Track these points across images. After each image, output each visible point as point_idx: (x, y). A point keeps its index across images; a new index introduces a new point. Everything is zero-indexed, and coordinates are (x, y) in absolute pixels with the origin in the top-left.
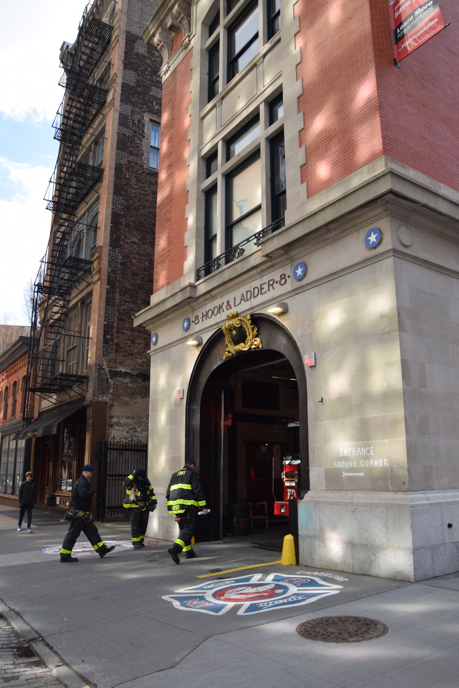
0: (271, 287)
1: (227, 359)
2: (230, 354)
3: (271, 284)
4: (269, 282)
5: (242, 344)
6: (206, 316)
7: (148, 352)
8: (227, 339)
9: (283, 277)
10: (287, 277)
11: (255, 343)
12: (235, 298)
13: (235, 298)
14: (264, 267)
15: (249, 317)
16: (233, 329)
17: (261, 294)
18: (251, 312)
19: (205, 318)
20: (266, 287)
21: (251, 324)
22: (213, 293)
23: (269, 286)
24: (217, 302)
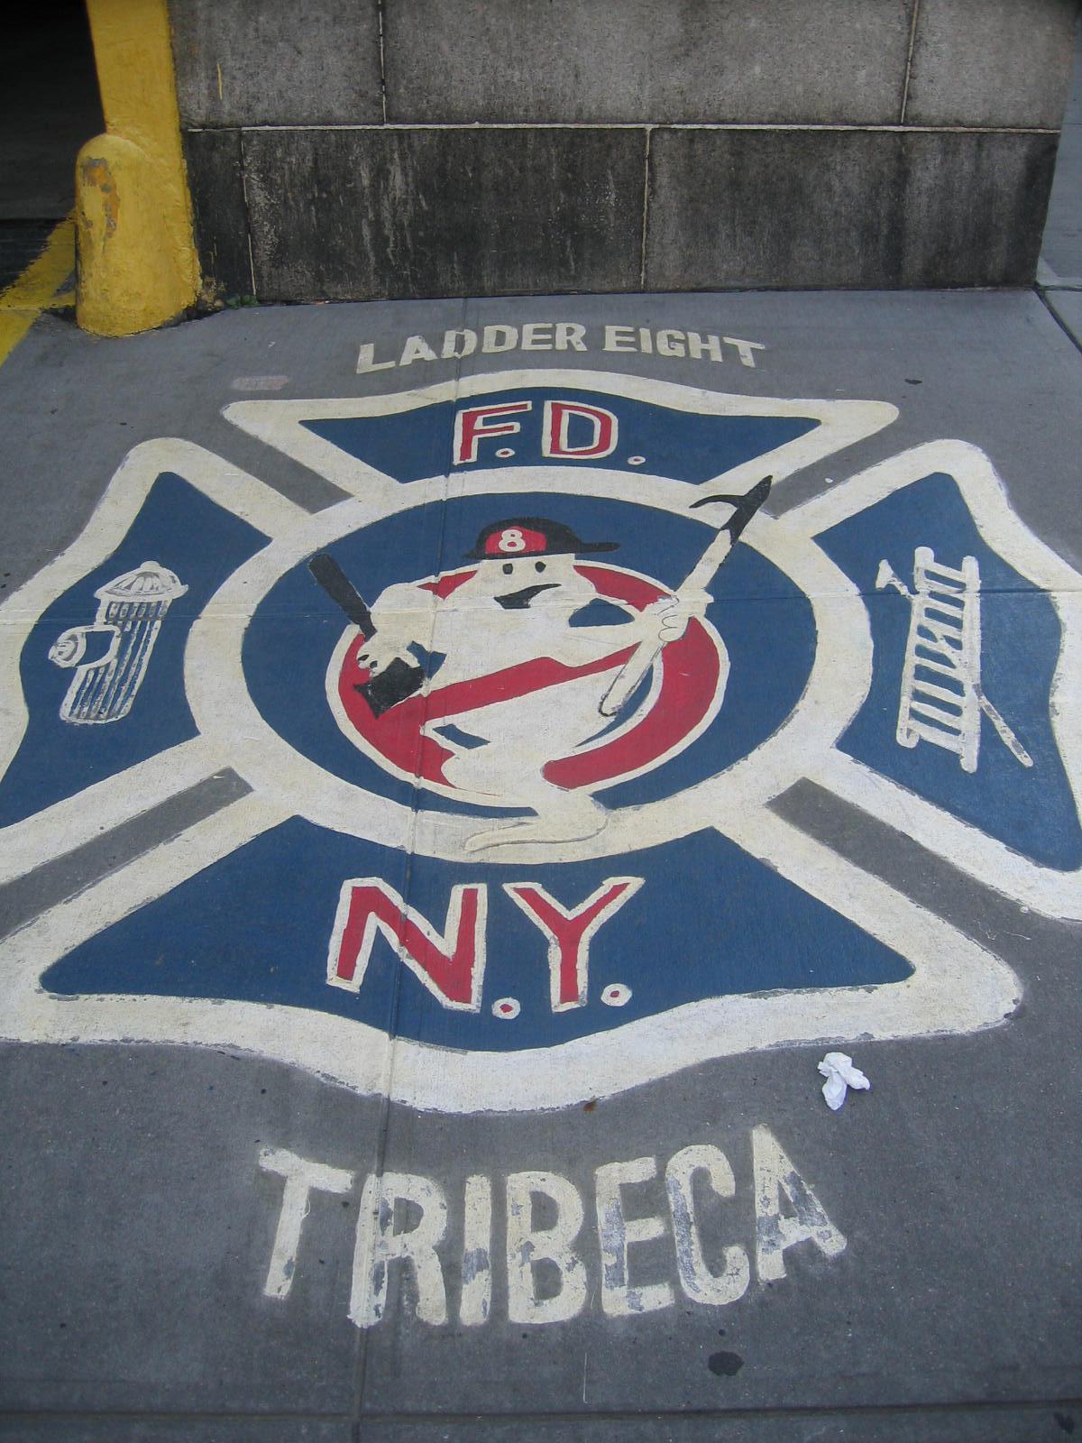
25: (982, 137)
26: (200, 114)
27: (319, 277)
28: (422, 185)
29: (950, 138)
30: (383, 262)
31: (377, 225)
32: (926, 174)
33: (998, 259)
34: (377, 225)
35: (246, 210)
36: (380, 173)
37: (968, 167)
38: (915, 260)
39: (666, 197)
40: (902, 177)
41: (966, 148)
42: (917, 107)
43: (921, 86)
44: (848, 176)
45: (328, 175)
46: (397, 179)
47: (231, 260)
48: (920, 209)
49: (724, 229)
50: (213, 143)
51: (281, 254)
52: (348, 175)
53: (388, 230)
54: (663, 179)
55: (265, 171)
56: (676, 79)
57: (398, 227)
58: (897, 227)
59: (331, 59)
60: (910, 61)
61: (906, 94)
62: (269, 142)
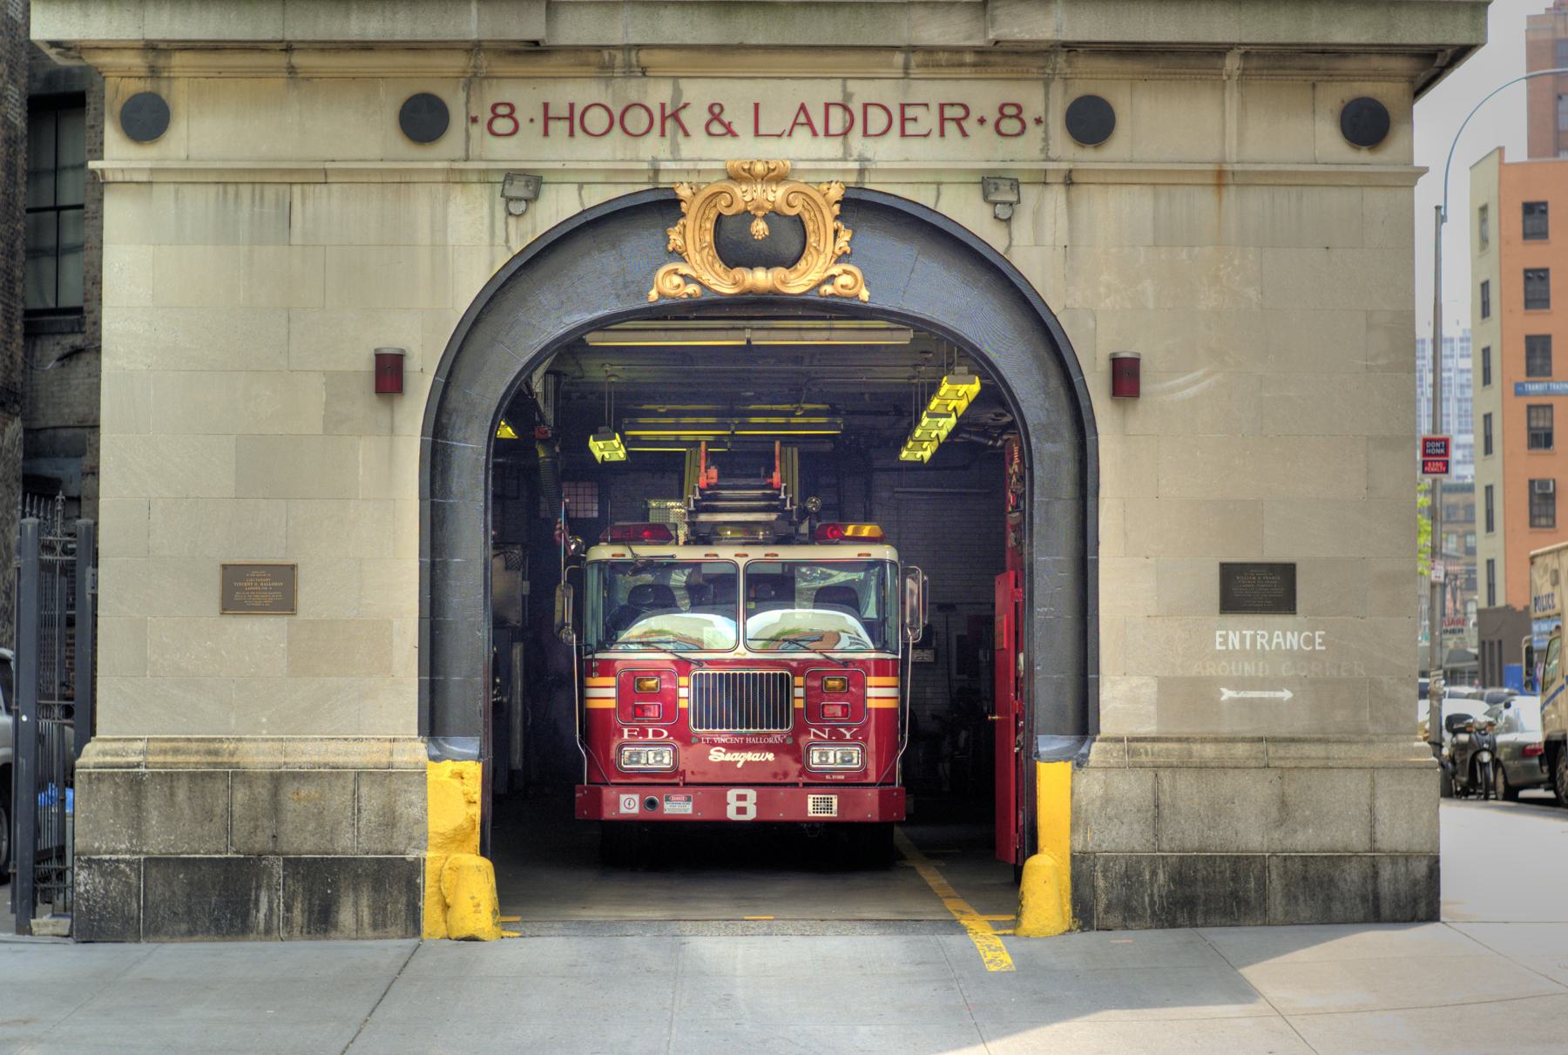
0: (951, 128)
1: (663, 302)
2: (692, 289)
3: (954, 118)
4: (942, 106)
5: (780, 272)
6: (575, 120)
7: (92, 165)
8: (692, 235)
9: (1010, 112)
10: (1028, 116)
11: (845, 280)
12: (757, 106)
13: (757, 106)
14: (943, 57)
15: (836, 192)
16: (760, 213)
17: (903, 134)
18: (852, 179)
19: (559, 128)
20: (928, 120)
21: (837, 218)
22: (644, 57)
23: (943, 120)
24: (658, 94)
25: (1408, 857)
26: (1078, 847)
27: (1125, 919)
28: (1172, 879)
29: (1394, 858)
30: (1154, 913)
31: (1151, 896)
32: (1386, 873)
33: (1422, 909)
34: (1151, 896)
35: (1094, 887)
36: (1154, 873)
37: (1403, 869)
38: (1386, 909)
39: (1276, 883)
40: (1376, 875)
41: (1401, 862)
42: (1378, 845)
43: (1379, 836)
44: (1353, 875)
45: (1130, 876)
46: (1161, 876)
47: (1084, 913)
48: (1385, 888)
49: (1302, 898)
50: (1083, 860)
51: (1109, 909)
52: (1140, 874)
53: (1156, 898)
54: (1274, 876)
55: (1105, 872)
56: (1276, 835)
57: (1161, 897)
58: (1376, 897)
59: (1135, 826)
60: (1372, 827)
61: (1373, 840)
62: (1107, 860)
